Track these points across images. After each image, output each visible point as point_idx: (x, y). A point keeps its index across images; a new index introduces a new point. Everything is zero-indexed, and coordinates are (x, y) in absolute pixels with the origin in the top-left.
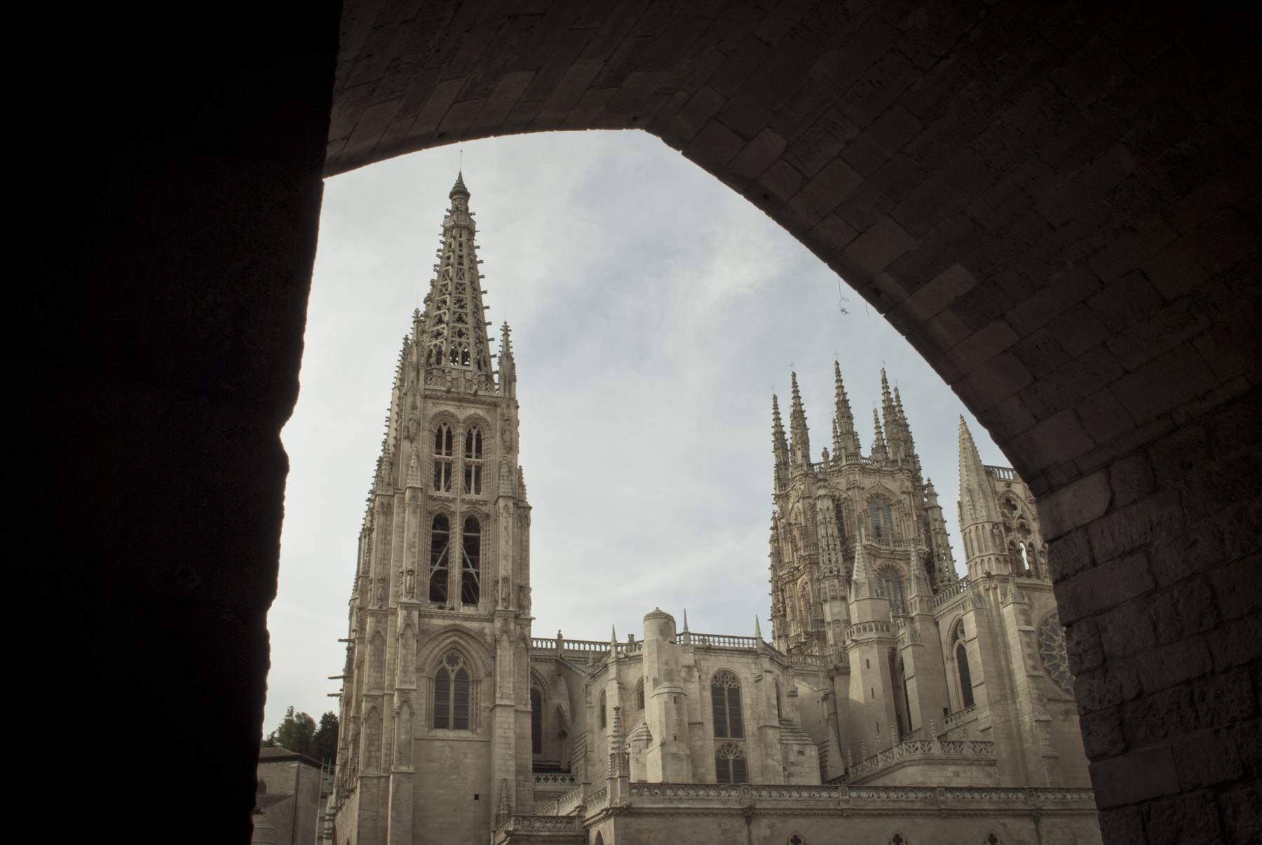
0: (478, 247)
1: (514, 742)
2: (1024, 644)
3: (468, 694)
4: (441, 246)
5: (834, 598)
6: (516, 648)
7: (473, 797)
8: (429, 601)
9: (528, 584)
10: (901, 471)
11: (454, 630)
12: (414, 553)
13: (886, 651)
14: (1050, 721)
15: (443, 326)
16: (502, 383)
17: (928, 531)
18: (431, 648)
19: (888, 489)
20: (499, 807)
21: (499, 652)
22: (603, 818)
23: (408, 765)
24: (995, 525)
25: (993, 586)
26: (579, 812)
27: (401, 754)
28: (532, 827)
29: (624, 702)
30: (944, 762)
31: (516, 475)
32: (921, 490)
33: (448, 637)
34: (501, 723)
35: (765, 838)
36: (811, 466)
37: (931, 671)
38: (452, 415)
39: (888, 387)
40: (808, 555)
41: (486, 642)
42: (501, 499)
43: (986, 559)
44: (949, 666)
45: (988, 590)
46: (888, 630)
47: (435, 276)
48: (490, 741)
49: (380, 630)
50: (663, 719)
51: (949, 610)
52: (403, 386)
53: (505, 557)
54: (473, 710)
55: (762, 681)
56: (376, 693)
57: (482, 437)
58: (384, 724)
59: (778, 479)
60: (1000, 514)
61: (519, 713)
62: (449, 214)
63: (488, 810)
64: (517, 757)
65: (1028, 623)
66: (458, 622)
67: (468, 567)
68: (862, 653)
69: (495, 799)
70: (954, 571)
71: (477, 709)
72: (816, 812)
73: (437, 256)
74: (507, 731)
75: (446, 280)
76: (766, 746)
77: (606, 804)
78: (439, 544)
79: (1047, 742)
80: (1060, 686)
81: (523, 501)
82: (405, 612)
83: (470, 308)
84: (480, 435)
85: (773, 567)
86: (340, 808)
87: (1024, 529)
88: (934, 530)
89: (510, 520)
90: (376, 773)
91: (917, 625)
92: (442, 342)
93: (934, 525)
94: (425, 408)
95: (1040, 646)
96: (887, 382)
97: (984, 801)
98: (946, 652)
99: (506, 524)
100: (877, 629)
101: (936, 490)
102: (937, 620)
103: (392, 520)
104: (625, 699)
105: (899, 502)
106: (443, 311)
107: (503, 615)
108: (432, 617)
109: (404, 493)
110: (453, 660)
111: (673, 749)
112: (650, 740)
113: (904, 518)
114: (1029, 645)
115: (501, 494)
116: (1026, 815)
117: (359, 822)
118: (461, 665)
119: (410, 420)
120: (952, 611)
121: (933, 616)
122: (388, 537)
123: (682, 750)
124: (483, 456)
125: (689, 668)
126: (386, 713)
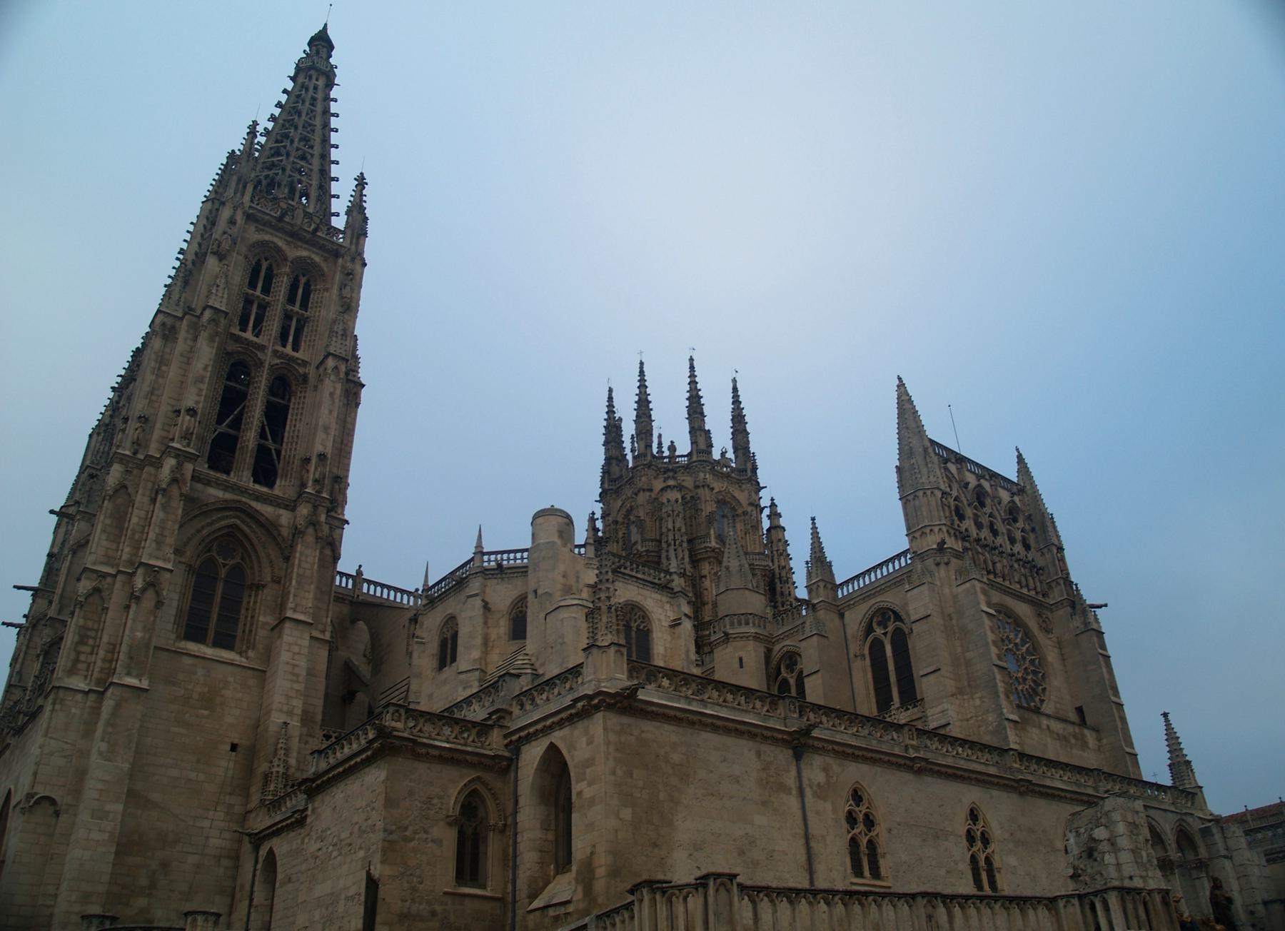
1: (304, 673)
2: (988, 628)
3: (241, 602)
7: (228, 747)
8: (206, 466)
9: (347, 476)
11: (236, 509)
13: (762, 650)
14: (1018, 722)
15: (280, 158)
16: (349, 233)
19: (734, 497)
20: (271, 762)
23: (139, 677)
25: (946, 560)
26: (499, 718)
27: (131, 658)
28: (420, 731)
29: (488, 628)
33: (227, 516)
34: (290, 644)
38: (279, 250)
40: (647, 551)
41: (280, 535)
45: (938, 564)
46: (765, 628)
48: (264, 672)
49: (127, 483)
51: (864, 599)
53: (326, 429)
54: (245, 625)
55: (682, 626)
58: (110, 614)
66: (244, 499)
71: (252, 625)
72: (882, 757)
74: (296, 657)
75: (292, 115)
84: (310, 286)
88: (777, 551)
89: (339, 386)
90: (83, 686)
92: (277, 174)
93: (777, 546)
98: (854, 648)
99: (332, 390)
100: (754, 624)
102: (842, 611)
104: (489, 625)
105: (745, 513)
107: (312, 501)
108: (208, 483)
115: (332, 350)
120: (867, 599)
122: (164, 368)
124: (309, 310)
126: (117, 596)
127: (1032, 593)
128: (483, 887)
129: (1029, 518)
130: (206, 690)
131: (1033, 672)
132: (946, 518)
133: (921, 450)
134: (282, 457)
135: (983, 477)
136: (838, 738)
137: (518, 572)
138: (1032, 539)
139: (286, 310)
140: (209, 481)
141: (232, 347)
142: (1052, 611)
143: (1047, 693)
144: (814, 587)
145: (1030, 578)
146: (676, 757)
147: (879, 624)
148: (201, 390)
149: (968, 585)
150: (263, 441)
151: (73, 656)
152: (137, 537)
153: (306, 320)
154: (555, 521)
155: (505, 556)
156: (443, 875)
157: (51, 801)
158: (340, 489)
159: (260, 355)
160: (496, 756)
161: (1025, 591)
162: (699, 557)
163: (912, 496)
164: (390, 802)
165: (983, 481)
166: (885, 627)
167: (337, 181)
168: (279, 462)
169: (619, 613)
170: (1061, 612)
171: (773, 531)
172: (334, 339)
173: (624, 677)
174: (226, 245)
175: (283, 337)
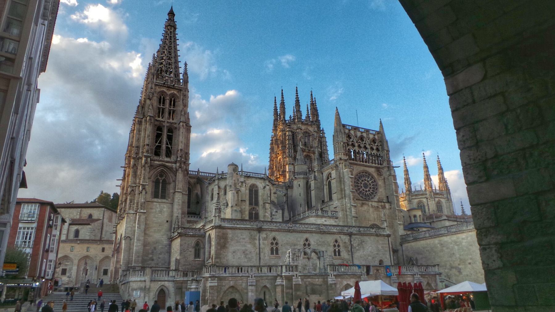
0: (177, 34)
4: (164, 32)
5: (290, 164)
6: (184, 173)
9: (189, 152)
12: (149, 139)
13: (305, 181)
15: (164, 61)
16: (183, 83)
17: (321, 145)
21: (178, 174)
22: (211, 229)
23: (144, 210)
24: (344, 143)
30: (322, 217)
31: (186, 114)
32: (320, 131)
35: (264, 238)
36: (286, 121)
37: (320, 189)
38: (165, 92)
39: (312, 97)
43: (340, 154)
44: (325, 187)
45: (340, 164)
46: (306, 175)
47: (161, 43)
49: (136, 164)
50: (233, 198)
52: (148, 80)
53: (182, 142)
55: (266, 189)
56: (134, 185)
57: (176, 101)
59: (274, 124)
60: (346, 140)
61: (184, 195)
62: (167, 21)
63: (171, 226)
64: (182, 209)
65: (352, 175)
67: (168, 145)
68: (298, 182)
69: (174, 222)
70: (328, 158)
73: (162, 35)
76: (266, 209)
77: (213, 225)
78: (158, 136)
79: (355, 212)
80: (360, 195)
81: (189, 124)
82: (145, 158)
83: (173, 55)
85: (270, 153)
86: (119, 223)
87: (353, 145)
89: (184, 130)
90: (133, 212)
91: (316, 174)
94: (155, 89)
95: (355, 182)
97: (335, 230)
98: (325, 183)
101: (325, 132)
103: (142, 127)
106: (163, 55)
108: (155, 161)
109: (147, 118)
111: (235, 208)
112: (227, 205)
114: (351, 182)
115: (182, 120)
116: (348, 234)
117: (126, 228)
122: (140, 133)
123: (238, 209)
125: (242, 182)
126: (137, 192)
127: (377, 165)
128: (200, 259)
131: (373, 188)
135: (364, 132)
136: (271, 227)
138: (380, 148)
141: (156, 123)
142: (383, 169)
148: (149, 139)
151: (130, 206)
152: (140, 177)
154: (232, 167)
156: (191, 258)
157: (130, 237)
159: (164, 124)
161: (374, 165)
164: (181, 245)
170: (385, 170)
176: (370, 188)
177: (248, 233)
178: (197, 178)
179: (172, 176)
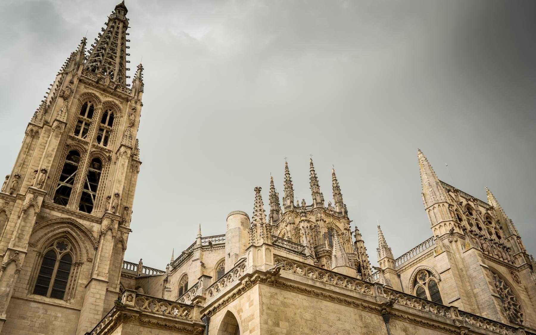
2: (485, 275)
3: (69, 274)
8: (53, 201)
10: (344, 218)
11: (68, 223)
15: (99, 57)
18: (46, 231)
25: (455, 239)
26: (198, 302)
38: (97, 97)
41: (93, 236)
42: (123, 147)
43: (448, 223)
45: (451, 242)
48: (80, 311)
49: (6, 209)
51: (411, 265)
54: (70, 285)
57: (115, 116)
61: (109, 293)
66: (73, 218)
71: (74, 285)
72: (440, 325)
74: (98, 301)
88: (361, 253)
96: (335, 175)
99: (123, 163)
102: (399, 274)
105: (343, 234)
107: (111, 217)
108: (53, 209)
110: (62, 246)
113: (346, 242)
115: (124, 143)
118: (68, 250)
119: (67, 87)
121: (396, 271)
122: (31, 152)
124: (113, 126)
129: (498, 222)
130: (44, 322)
132: (452, 217)
133: (435, 184)
134: (96, 198)
135: (470, 200)
137: (220, 247)
139: (101, 126)
140: (53, 208)
141: (70, 142)
142: (518, 271)
143: (524, 316)
144: (382, 261)
145: (504, 253)
146: (308, 316)
147: (421, 278)
149: (470, 251)
150: (86, 191)
153: (111, 131)
155: (213, 239)
158: (127, 213)
160: (194, 325)
162: (320, 256)
163: (432, 207)
165: (470, 202)
166: (424, 280)
167: (129, 70)
168: (94, 200)
169: (268, 227)
170: (524, 272)
171: (357, 243)
172: (125, 138)
173: (272, 263)
174: (67, 93)
175: (99, 139)
176: (509, 303)
177: (357, 317)
178: (136, 278)
179: (88, 248)
